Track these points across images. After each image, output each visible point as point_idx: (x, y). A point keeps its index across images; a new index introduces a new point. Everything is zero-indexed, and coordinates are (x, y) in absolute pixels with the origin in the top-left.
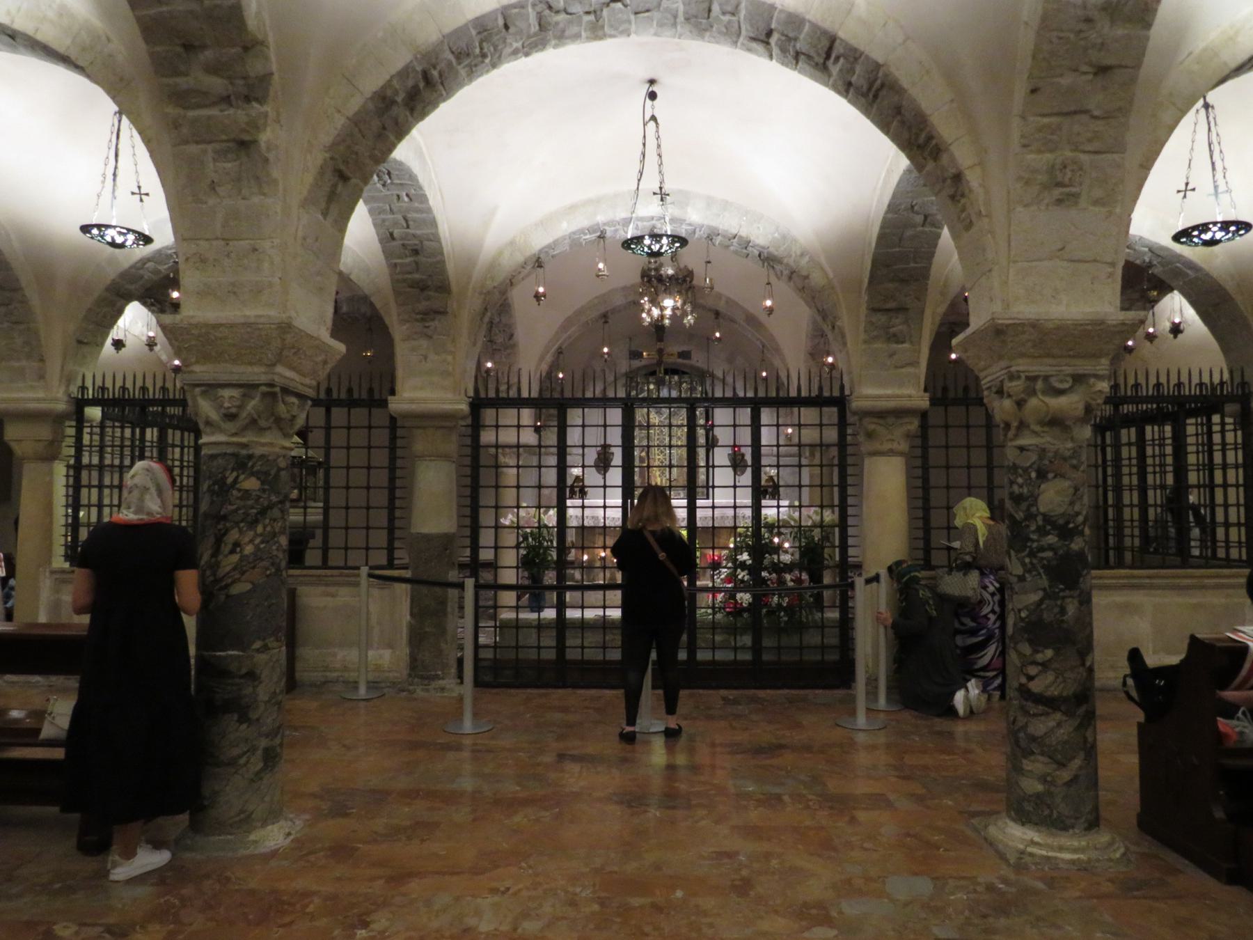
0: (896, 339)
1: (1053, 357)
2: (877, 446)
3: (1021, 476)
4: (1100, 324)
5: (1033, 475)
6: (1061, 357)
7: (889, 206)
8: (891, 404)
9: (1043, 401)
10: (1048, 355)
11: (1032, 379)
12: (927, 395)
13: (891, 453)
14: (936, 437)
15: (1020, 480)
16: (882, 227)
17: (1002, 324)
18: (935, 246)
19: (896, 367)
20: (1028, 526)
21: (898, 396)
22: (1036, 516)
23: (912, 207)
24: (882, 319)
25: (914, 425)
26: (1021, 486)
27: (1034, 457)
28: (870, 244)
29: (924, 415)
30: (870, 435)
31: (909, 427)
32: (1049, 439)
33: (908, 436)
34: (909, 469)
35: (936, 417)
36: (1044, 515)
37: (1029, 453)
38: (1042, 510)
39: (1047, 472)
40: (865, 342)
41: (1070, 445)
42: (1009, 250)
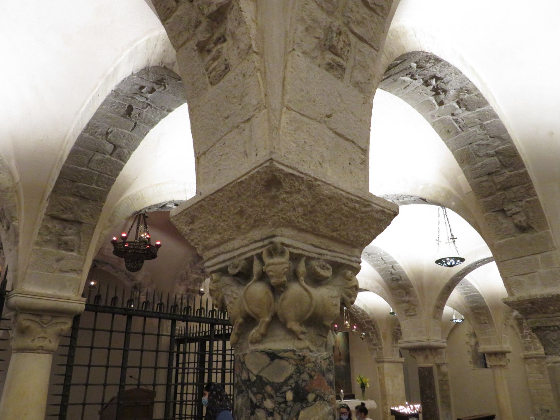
2: (28, 342)
3: (271, 397)
4: (366, 206)
5: (290, 396)
6: (324, 237)
7: (88, 125)
10: (315, 233)
11: (295, 258)
12: (85, 299)
13: (41, 350)
14: (83, 338)
15: (269, 404)
16: (77, 144)
17: (280, 171)
18: (117, 175)
21: (59, 297)
23: (107, 133)
24: (57, 226)
25: (66, 326)
27: (290, 369)
28: (61, 159)
29: (77, 318)
30: (23, 331)
31: (63, 327)
33: (60, 335)
34: (55, 366)
35: (87, 321)
37: (284, 363)
39: (308, 393)
40: (37, 243)
41: (325, 354)
42: (283, 95)
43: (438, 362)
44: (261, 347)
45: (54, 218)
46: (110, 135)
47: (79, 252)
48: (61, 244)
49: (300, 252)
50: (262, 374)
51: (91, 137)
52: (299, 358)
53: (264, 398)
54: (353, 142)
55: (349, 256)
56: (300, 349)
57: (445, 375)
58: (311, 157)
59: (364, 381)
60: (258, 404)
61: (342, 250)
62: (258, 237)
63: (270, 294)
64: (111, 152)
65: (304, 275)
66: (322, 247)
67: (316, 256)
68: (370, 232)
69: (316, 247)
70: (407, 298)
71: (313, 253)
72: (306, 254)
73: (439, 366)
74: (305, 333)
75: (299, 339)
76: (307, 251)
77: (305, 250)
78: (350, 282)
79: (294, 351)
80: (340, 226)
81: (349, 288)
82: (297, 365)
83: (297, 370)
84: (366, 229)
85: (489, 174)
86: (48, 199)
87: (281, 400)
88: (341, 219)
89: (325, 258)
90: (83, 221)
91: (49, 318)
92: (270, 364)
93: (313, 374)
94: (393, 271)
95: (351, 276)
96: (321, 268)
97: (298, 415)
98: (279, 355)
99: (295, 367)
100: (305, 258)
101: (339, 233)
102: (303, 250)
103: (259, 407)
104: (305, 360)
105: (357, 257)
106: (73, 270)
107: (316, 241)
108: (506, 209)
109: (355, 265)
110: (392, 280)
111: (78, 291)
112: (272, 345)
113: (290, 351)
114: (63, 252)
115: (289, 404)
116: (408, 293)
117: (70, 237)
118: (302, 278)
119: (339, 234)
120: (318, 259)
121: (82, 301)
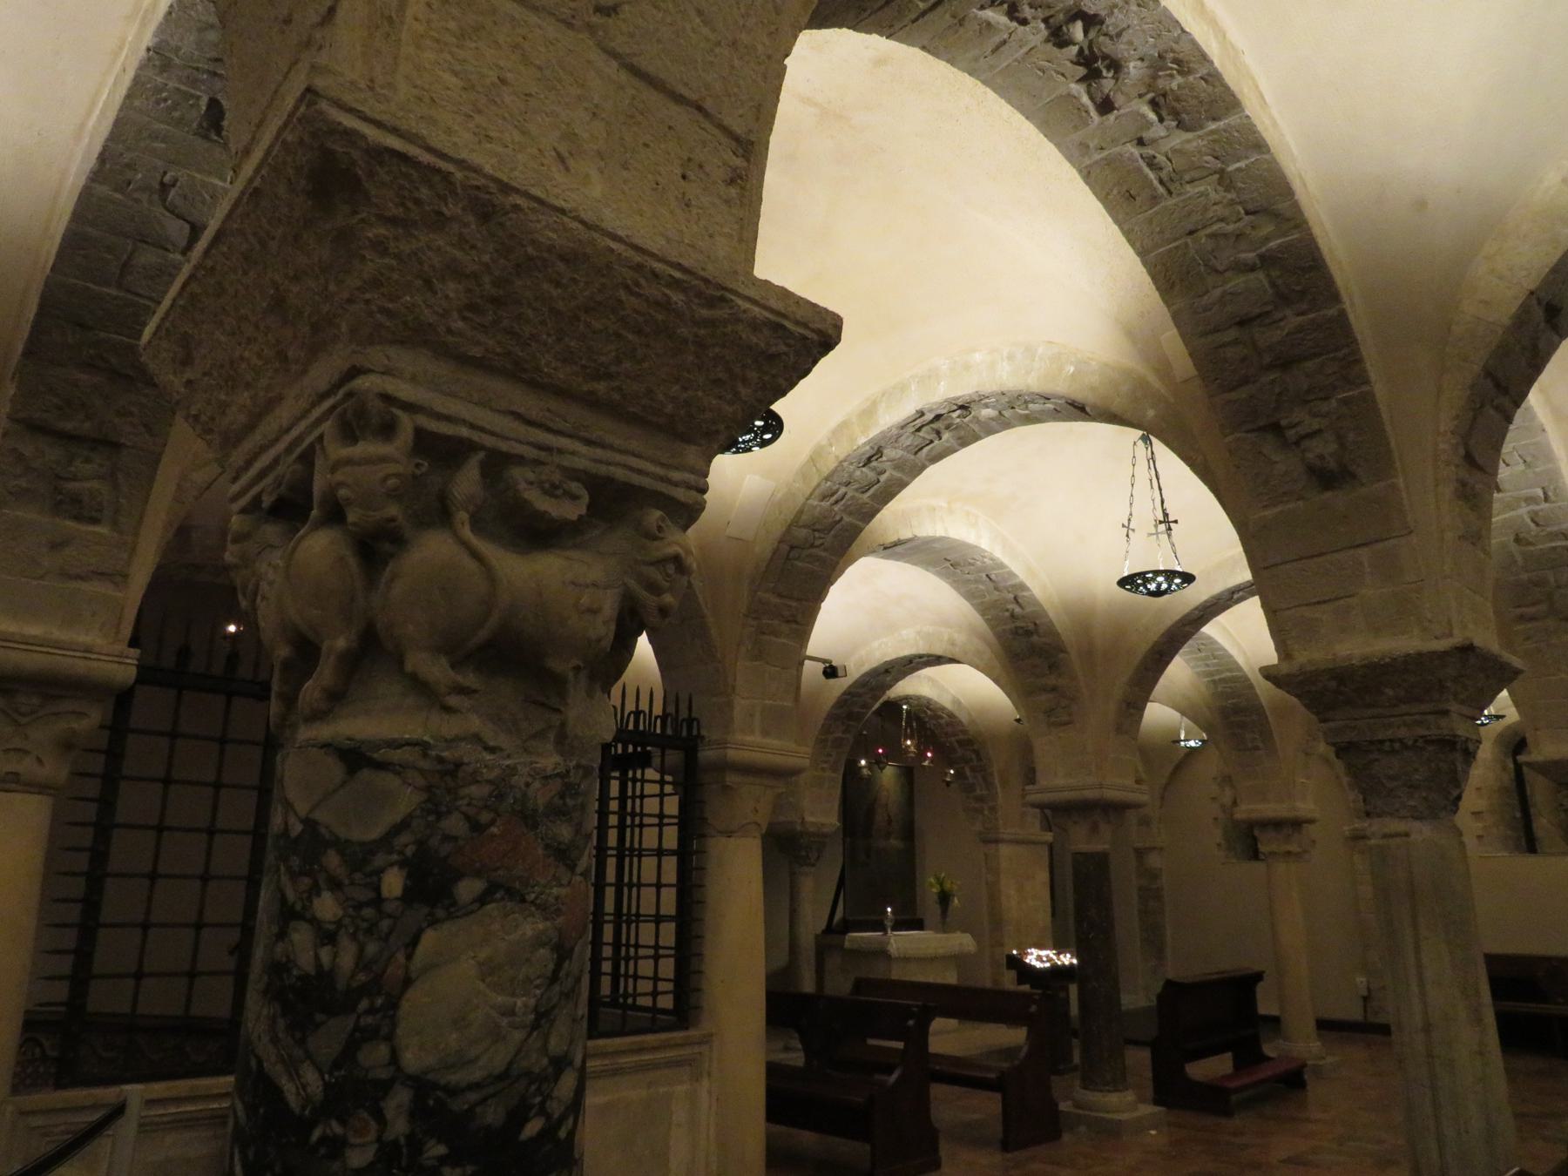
0: (79, 508)
1: (536, 385)
3: (335, 885)
4: (712, 303)
5: (393, 883)
7: (103, 158)
8: (33, 661)
9: (476, 555)
10: (520, 373)
12: (135, 652)
15: (327, 907)
16: (78, 216)
17: (350, 135)
19: (66, 575)
20: (336, 1147)
21: (58, 645)
22: (385, 1087)
25: (89, 720)
26: (327, 937)
27: (406, 800)
29: (123, 699)
31: (75, 725)
32: (475, 723)
33: (67, 745)
36: (421, 1085)
37: (389, 781)
38: (412, 1060)
39: (459, 876)
41: (550, 761)
43: (1139, 845)
44: (324, 731)
45: (36, 428)
46: (173, 192)
47: (115, 524)
48: (61, 502)
49: (464, 432)
50: (318, 816)
51: (118, 196)
52: (439, 767)
53: (315, 890)
54: (700, 109)
55: (662, 465)
56: (446, 741)
57: (1154, 875)
58: (524, 133)
59: (947, 886)
60: (298, 907)
61: (634, 445)
62: (323, 385)
63: (353, 562)
64: (183, 243)
65: (471, 508)
66: (551, 425)
67: (531, 452)
68: (736, 394)
69: (530, 423)
70: (1052, 680)
71: (521, 442)
72: (489, 441)
73: (1140, 853)
74: (475, 691)
75: (448, 709)
76: (492, 434)
77: (482, 430)
78: (656, 543)
79: (423, 746)
80: (618, 361)
81: (652, 564)
82: (429, 789)
83: (430, 806)
84: (717, 382)
85: (1243, 323)
86: (14, 374)
87: (365, 895)
88: (619, 336)
89: (566, 464)
90: (122, 441)
91: (35, 701)
92: (343, 784)
93: (485, 817)
94: (1017, 610)
95: (660, 528)
96: (546, 492)
97: (414, 942)
98: (375, 756)
99: (424, 796)
100: (481, 455)
101: (616, 383)
102: (473, 426)
103: (299, 916)
104: (460, 774)
105: (692, 471)
106: (101, 575)
107: (529, 403)
108: (1284, 423)
109: (680, 494)
110: (1016, 632)
111: (117, 633)
112: (355, 726)
113: (409, 743)
114: (70, 523)
115: (389, 907)
116: (1053, 667)
117: (87, 485)
118: (462, 516)
119: (620, 389)
120: (537, 462)
121: (127, 657)
